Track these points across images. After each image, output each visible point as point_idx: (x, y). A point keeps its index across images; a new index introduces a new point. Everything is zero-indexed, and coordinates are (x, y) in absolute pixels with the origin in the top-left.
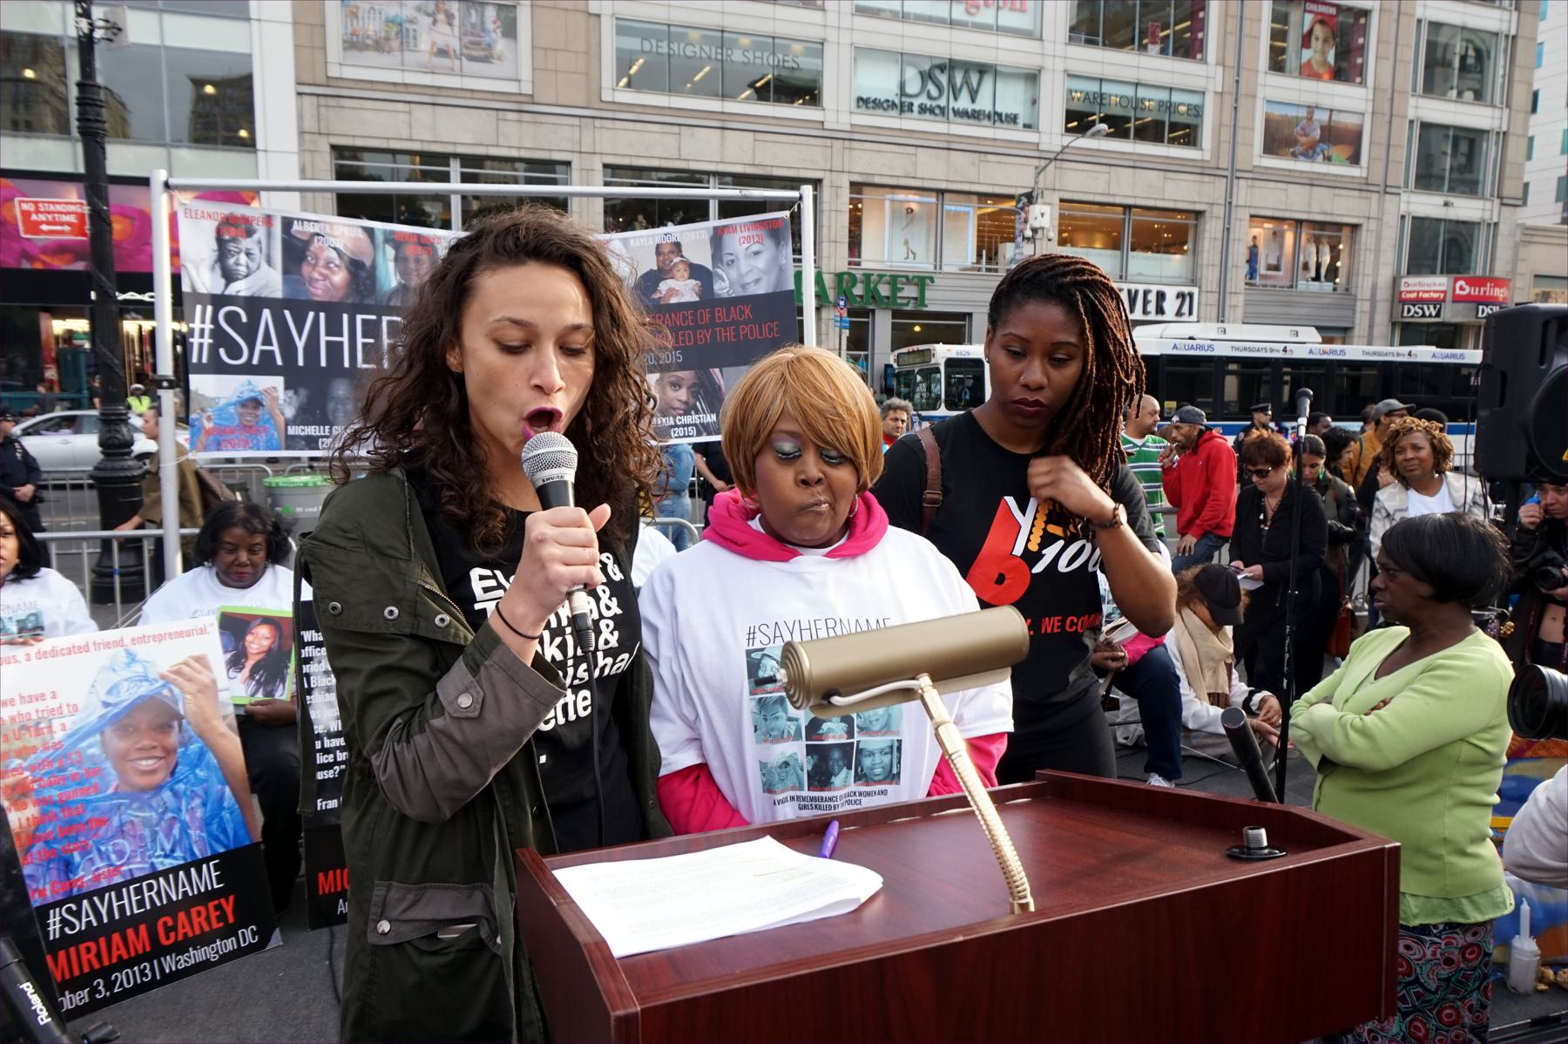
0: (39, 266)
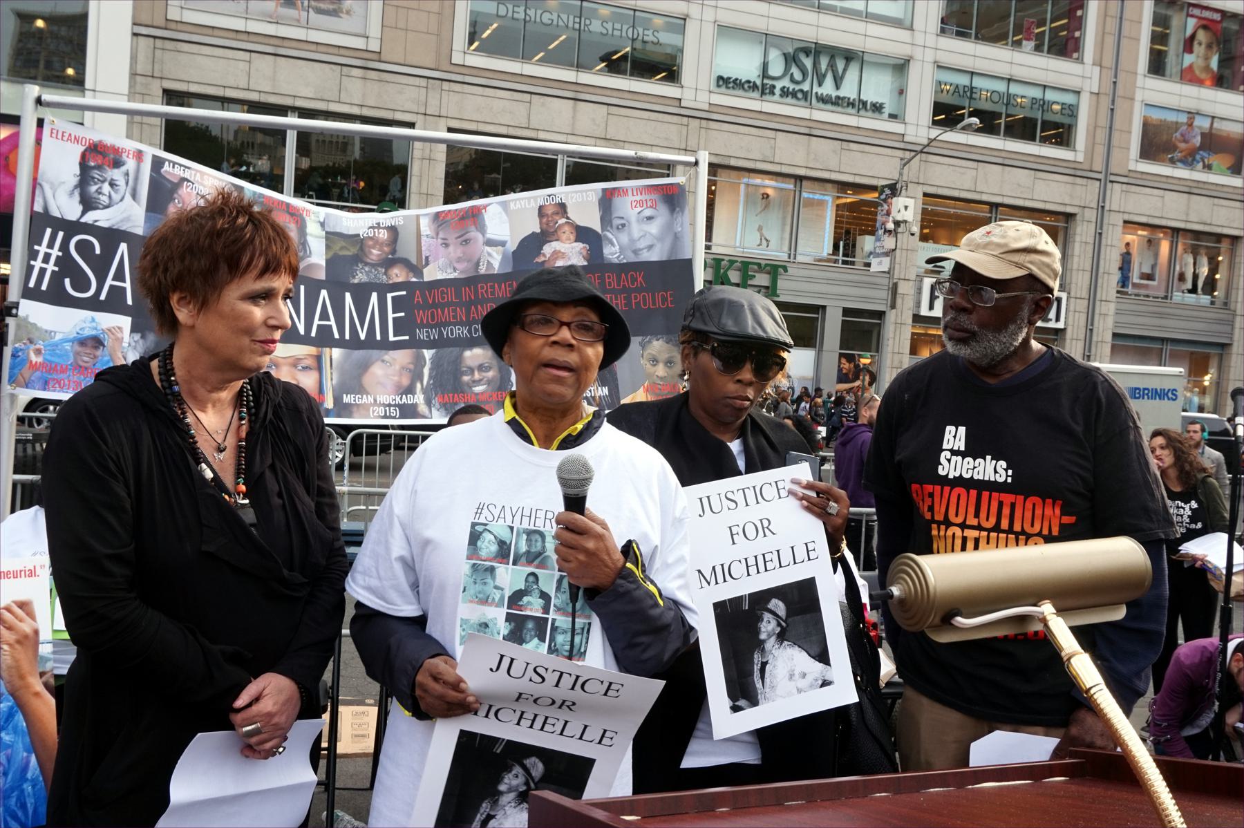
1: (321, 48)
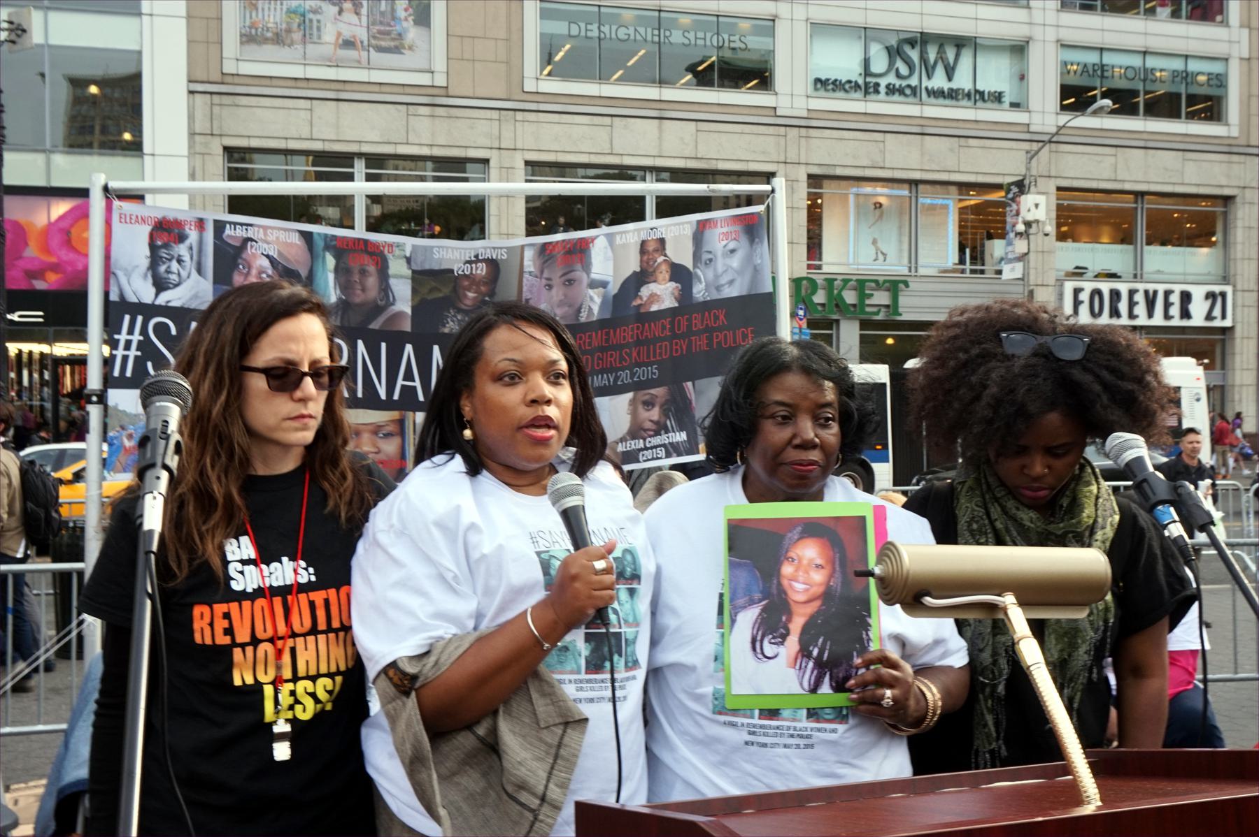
1: (384, 89)
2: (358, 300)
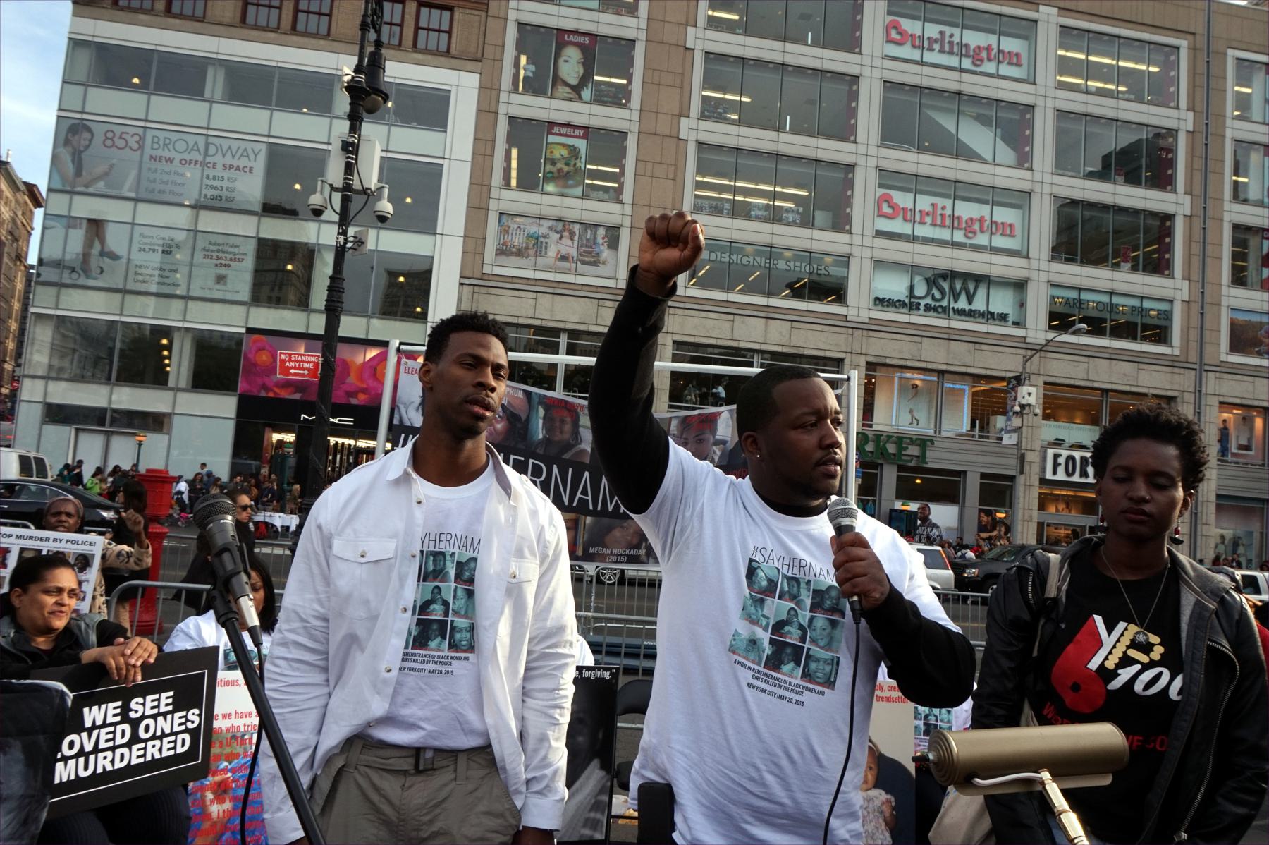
0: (271, 395)
2: (556, 439)
